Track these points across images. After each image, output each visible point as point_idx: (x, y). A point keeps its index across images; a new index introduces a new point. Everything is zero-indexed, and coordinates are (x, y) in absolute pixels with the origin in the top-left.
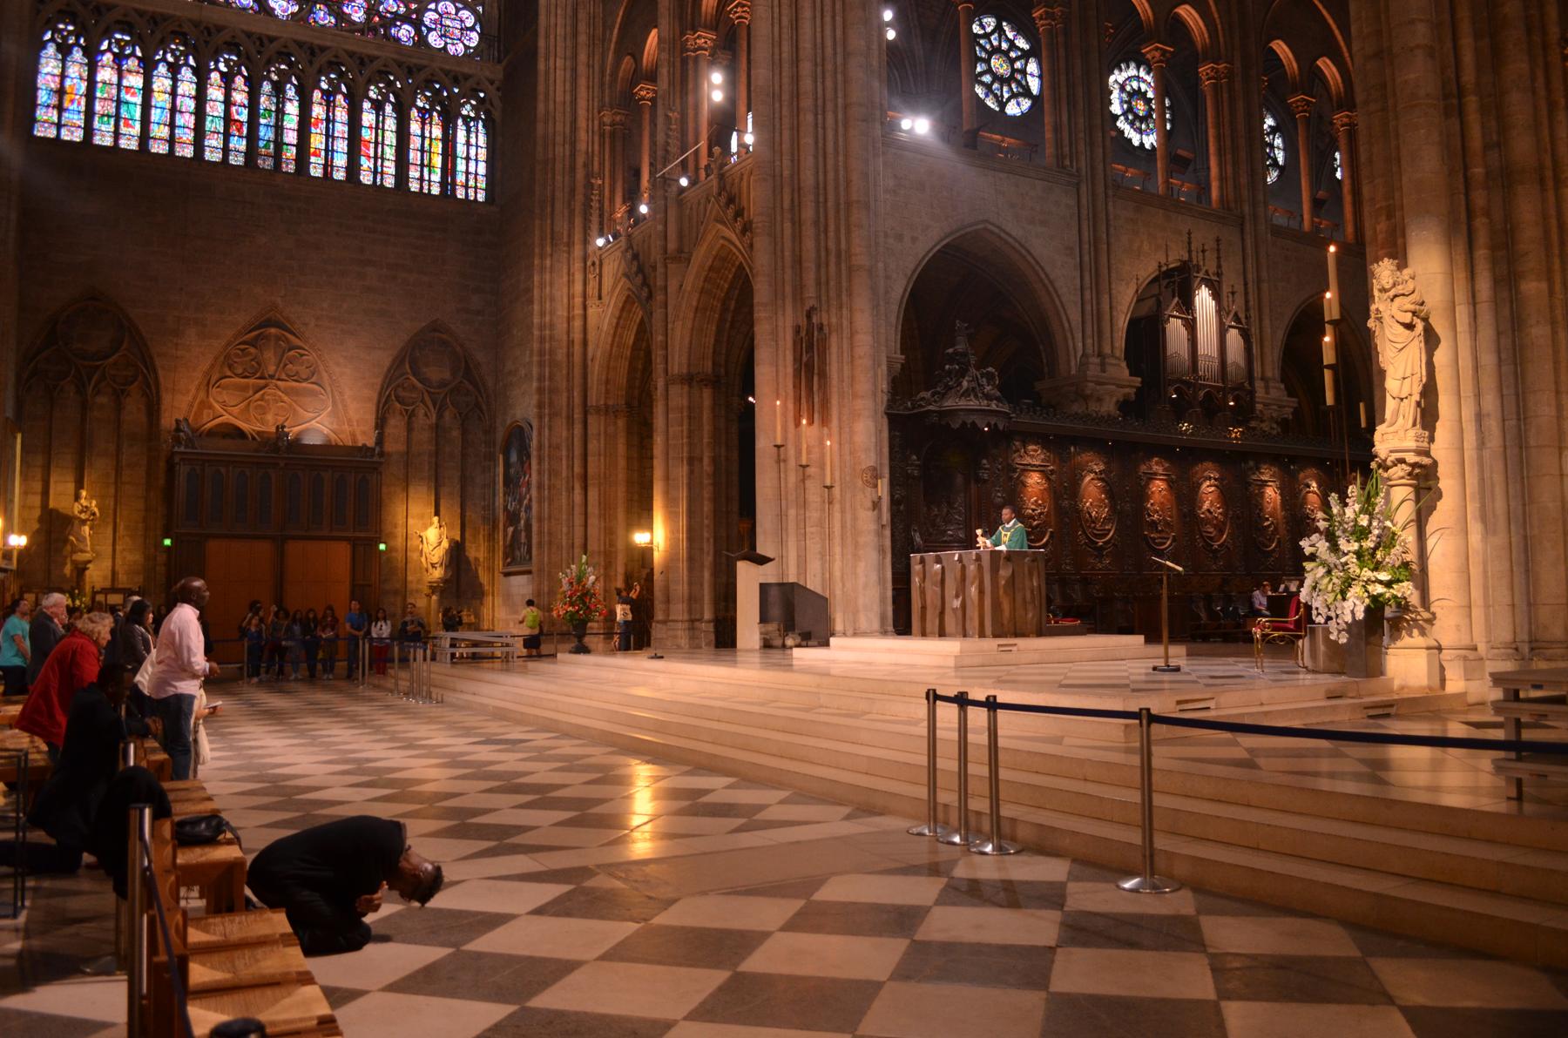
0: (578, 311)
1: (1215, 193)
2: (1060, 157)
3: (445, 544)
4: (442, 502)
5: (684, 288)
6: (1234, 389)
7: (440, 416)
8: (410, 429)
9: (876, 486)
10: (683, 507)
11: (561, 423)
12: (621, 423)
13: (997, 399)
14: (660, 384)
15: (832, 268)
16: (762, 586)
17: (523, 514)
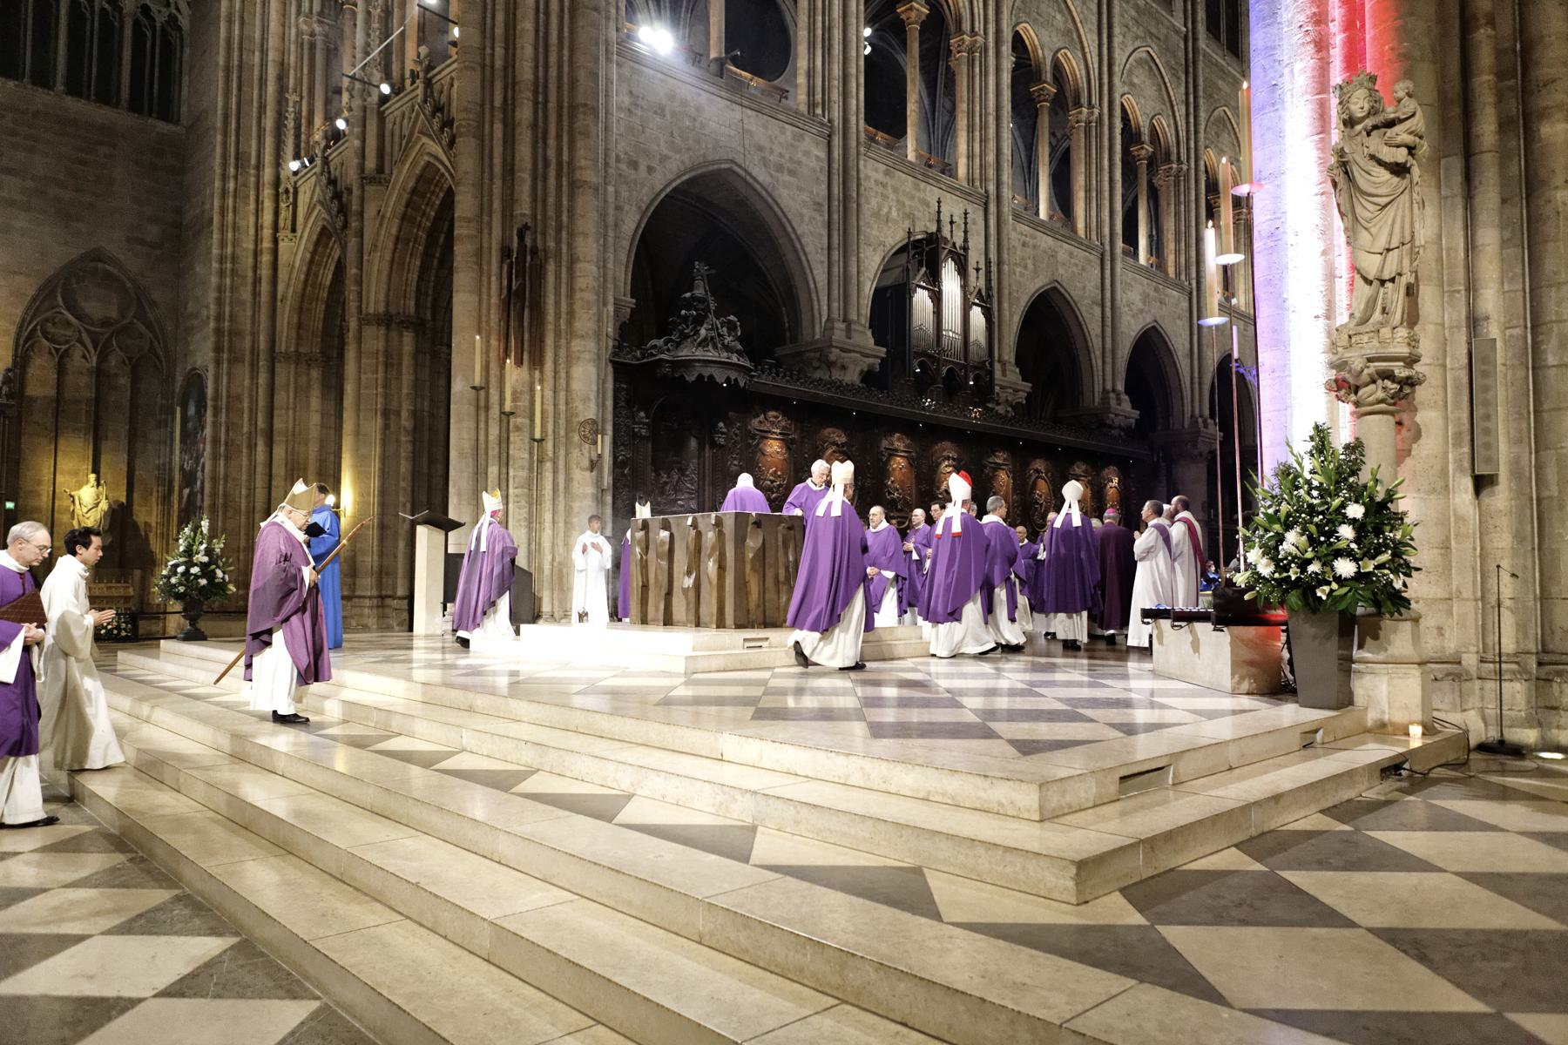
0: (267, 244)
1: (962, 170)
2: (812, 105)
3: (104, 505)
4: (105, 459)
5: (381, 214)
6: (975, 368)
7: (103, 358)
8: (61, 370)
9: (595, 443)
10: (375, 466)
11: (243, 372)
12: (315, 374)
13: (738, 352)
14: (353, 324)
15: (552, 181)
16: (448, 556)
17: (199, 474)
